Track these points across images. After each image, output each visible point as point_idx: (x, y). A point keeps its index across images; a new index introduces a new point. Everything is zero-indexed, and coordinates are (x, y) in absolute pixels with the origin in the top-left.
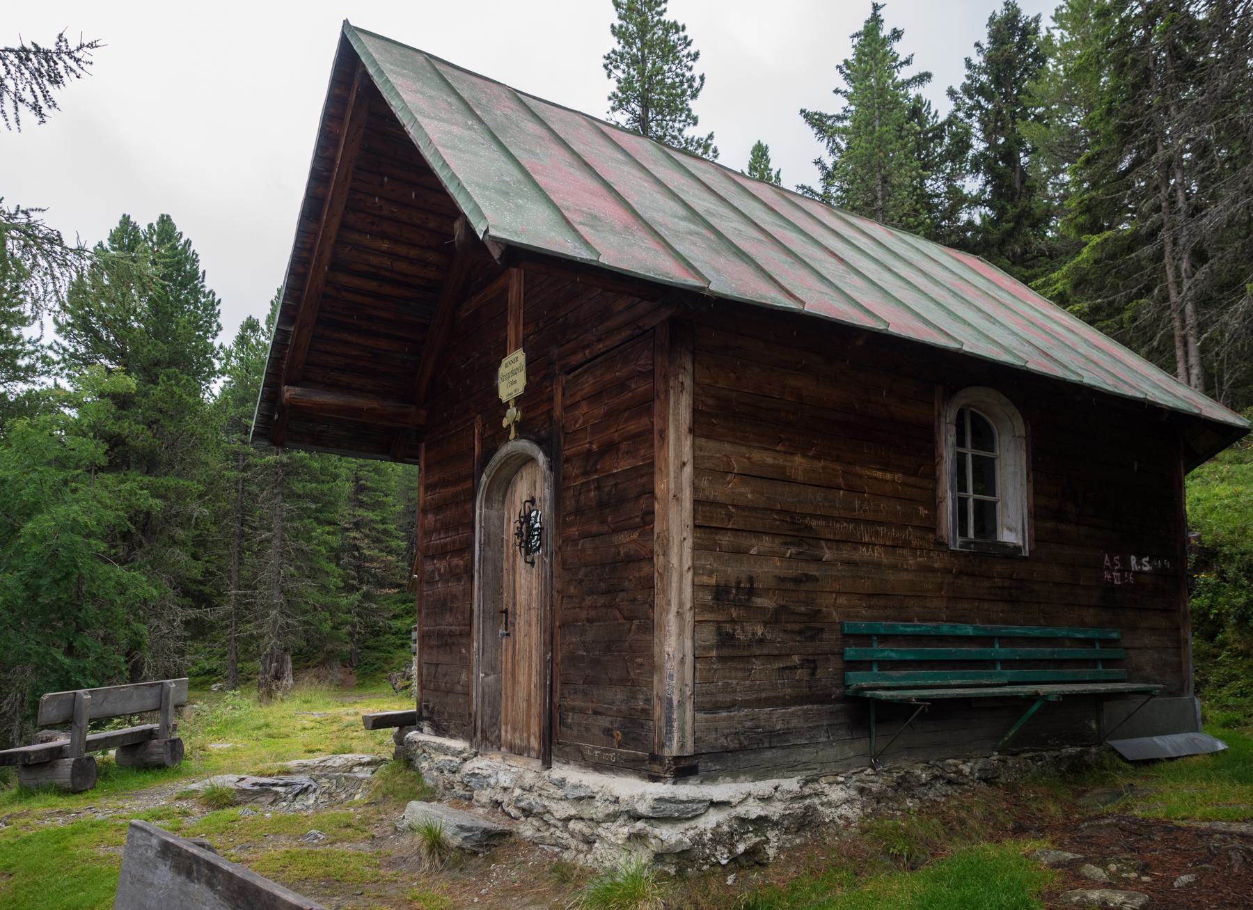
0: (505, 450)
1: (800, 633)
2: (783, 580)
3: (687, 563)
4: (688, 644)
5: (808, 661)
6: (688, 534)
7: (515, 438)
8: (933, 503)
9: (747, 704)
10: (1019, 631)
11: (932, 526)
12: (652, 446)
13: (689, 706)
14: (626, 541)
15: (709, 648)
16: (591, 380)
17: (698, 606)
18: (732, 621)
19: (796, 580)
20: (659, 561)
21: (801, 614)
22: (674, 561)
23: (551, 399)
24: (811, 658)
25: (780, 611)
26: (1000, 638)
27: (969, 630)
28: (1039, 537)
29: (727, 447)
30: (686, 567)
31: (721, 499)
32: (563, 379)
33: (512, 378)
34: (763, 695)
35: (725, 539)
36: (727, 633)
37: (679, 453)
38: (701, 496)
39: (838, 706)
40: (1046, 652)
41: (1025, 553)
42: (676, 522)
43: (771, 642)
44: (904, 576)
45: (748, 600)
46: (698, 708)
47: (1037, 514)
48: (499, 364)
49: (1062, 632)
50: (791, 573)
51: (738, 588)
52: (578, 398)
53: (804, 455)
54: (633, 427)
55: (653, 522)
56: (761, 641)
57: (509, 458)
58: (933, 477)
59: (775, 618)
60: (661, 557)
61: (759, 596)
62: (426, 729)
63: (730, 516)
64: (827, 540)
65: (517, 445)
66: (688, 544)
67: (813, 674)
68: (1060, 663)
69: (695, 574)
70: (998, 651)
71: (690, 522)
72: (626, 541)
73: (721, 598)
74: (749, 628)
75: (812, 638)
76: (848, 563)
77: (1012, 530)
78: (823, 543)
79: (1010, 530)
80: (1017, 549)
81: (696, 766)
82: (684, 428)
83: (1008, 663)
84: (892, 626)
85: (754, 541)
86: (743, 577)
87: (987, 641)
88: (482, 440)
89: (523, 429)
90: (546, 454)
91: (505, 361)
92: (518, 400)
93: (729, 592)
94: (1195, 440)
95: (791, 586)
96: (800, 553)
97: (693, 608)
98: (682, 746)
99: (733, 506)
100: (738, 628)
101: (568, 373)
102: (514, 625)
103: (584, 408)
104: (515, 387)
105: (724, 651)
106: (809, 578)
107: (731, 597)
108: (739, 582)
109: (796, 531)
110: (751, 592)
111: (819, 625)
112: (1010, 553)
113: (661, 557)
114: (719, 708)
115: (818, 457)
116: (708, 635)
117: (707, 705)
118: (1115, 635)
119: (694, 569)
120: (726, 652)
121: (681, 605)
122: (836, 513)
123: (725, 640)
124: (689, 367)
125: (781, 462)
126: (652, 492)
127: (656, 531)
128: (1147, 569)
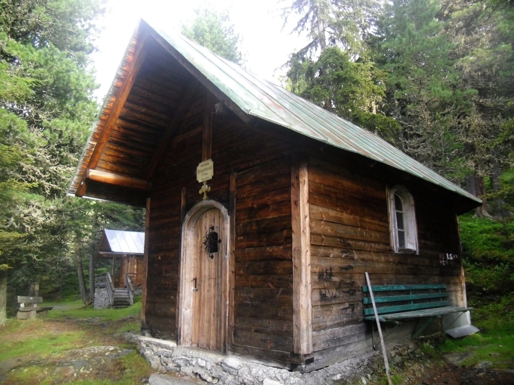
0: (200, 204)
1: (348, 292)
2: (342, 268)
3: (308, 262)
4: (310, 301)
5: (351, 305)
6: (308, 248)
7: (206, 199)
8: (388, 233)
9: (331, 327)
10: (418, 287)
11: (388, 243)
12: (290, 207)
13: (310, 329)
14: (277, 250)
15: (317, 301)
16: (253, 176)
17: (313, 283)
18: (325, 288)
19: (346, 268)
20: (295, 261)
21: (348, 284)
22: (303, 261)
23: (228, 183)
24: (352, 303)
25: (341, 282)
26: (412, 290)
27: (402, 288)
28: (421, 246)
29: (321, 209)
30: (308, 264)
31: (319, 232)
32: (235, 174)
33: (205, 172)
34: (336, 322)
35: (322, 251)
36: (323, 294)
37: (304, 211)
38: (313, 231)
39: (361, 325)
40: (425, 295)
41: (418, 254)
42: (303, 242)
43: (339, 297)
44: (381, 265)
45: (330, 278)
46: (314, 330)
47: (421, 236)
48: (197, 165)
49: (430, 287)
50: (345, 265)
51: (326, 273)
52: (245, 183)
53: (347, 213)
54: (278, 198)
55: (291, 243)
56: (335, 297)
57: (203, 207)
58: (387, 222)
59: (339, 286)
60: (297, 259)
61: (334, 276)
62: (147, 334)
63: (323, 240)
64: (355, 250)
65: (206, 202)
66: (309, 253)
67: (353, 310)
68: (429, 300)
69: (312, 267)
70: (412, 296)
71: (309, 243)
72: (277, 250)
73: (322, 277)
74: (331, 291)
75: (352, 294)
76: (363, 260)
77: (412, 244)
78: (354, 251)
79: (411, 244)
80: (415, 252)
81: (313, 358)
82: (306, 200)
83: (415, 301)
84: (379, 287)
85: (331, 251)
86: (328, 268)
87: (407, 292)
88: (186, 197)
89: (210, 195)
90: (226, 207)
91: (200, 164)
92: (209, 182)
93: (323, 275)
94: (469, 206)
95: (344, 271)
96: (347, 256)
97: (311, 283)
98: (308, 349)
99: (324, 235)
100: (327, 291)
101: (238, 172)
102: (200, 285)
103: (248, 188)
104: (207, 176)
105: (324, 301)
106: (350, 267)
107: (324, 277)
108: (327, 270)
109: (345, 245)
110: (331, 275)
111: (353, 288)
112: (410, 254)
113: (297, 259)
114: (321, 329)
115: (351, 214)
116: (317, 296)
117: (317, 328)
118: (445, 287)
119: (312, 265)
120: (323, 303)
121: (306, 282)
122: (358, 238)
123: (323, 297)
124: (307, 174)
125: (339, 215)
126: (291, 228)
127: (293, 247)
128: (451, 258)
